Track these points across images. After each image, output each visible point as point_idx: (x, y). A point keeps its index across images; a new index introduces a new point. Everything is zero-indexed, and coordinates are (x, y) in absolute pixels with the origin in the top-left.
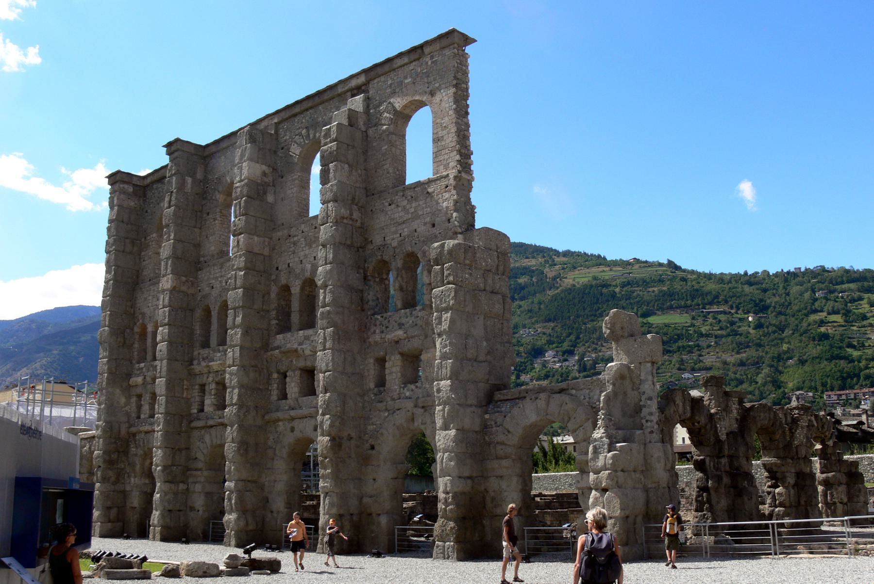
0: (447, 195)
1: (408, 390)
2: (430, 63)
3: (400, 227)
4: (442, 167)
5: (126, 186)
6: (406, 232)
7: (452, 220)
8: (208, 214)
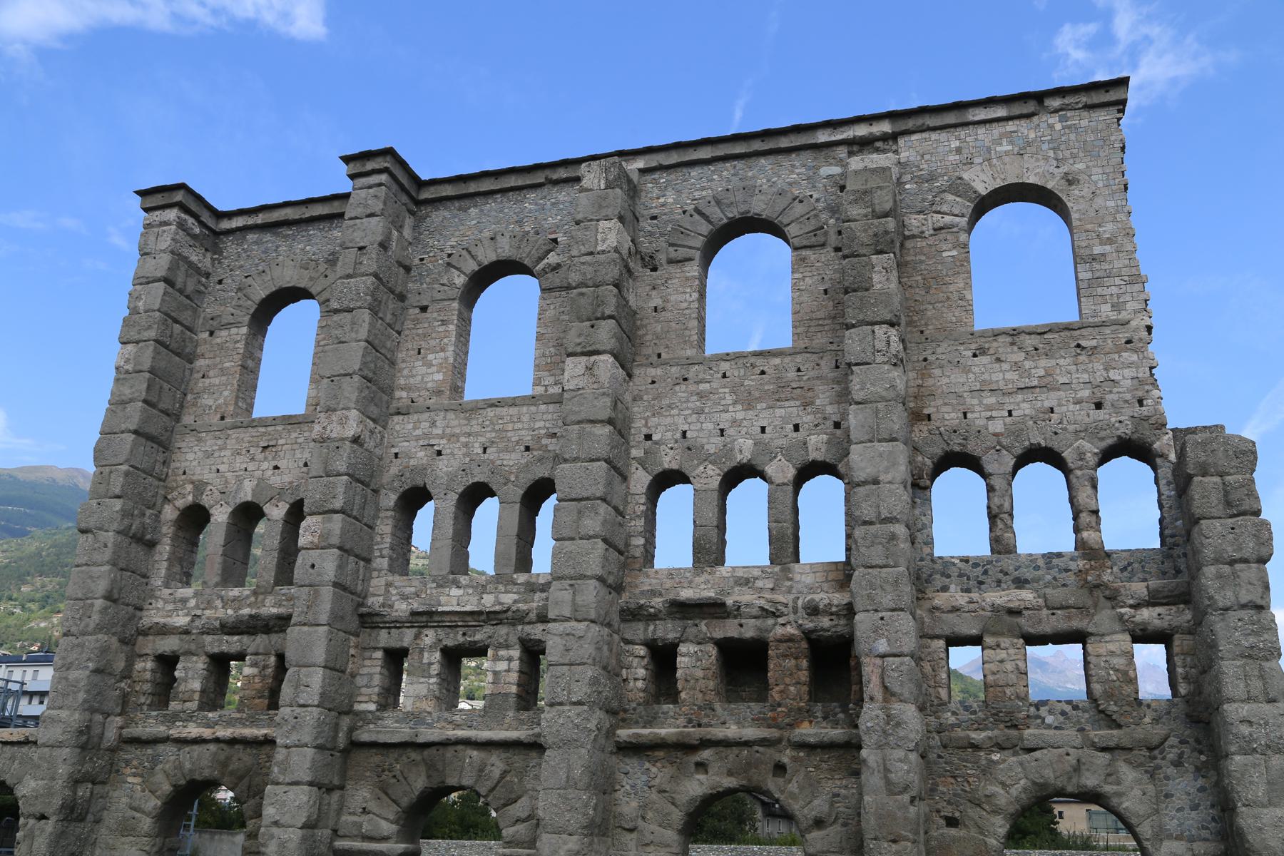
1: (1050, 712)
2: (1058, 126)
3: (1006, 399)
5: (191, 220)
6: (1026, 409)
7: (1148, 402)
8: (424, 309)
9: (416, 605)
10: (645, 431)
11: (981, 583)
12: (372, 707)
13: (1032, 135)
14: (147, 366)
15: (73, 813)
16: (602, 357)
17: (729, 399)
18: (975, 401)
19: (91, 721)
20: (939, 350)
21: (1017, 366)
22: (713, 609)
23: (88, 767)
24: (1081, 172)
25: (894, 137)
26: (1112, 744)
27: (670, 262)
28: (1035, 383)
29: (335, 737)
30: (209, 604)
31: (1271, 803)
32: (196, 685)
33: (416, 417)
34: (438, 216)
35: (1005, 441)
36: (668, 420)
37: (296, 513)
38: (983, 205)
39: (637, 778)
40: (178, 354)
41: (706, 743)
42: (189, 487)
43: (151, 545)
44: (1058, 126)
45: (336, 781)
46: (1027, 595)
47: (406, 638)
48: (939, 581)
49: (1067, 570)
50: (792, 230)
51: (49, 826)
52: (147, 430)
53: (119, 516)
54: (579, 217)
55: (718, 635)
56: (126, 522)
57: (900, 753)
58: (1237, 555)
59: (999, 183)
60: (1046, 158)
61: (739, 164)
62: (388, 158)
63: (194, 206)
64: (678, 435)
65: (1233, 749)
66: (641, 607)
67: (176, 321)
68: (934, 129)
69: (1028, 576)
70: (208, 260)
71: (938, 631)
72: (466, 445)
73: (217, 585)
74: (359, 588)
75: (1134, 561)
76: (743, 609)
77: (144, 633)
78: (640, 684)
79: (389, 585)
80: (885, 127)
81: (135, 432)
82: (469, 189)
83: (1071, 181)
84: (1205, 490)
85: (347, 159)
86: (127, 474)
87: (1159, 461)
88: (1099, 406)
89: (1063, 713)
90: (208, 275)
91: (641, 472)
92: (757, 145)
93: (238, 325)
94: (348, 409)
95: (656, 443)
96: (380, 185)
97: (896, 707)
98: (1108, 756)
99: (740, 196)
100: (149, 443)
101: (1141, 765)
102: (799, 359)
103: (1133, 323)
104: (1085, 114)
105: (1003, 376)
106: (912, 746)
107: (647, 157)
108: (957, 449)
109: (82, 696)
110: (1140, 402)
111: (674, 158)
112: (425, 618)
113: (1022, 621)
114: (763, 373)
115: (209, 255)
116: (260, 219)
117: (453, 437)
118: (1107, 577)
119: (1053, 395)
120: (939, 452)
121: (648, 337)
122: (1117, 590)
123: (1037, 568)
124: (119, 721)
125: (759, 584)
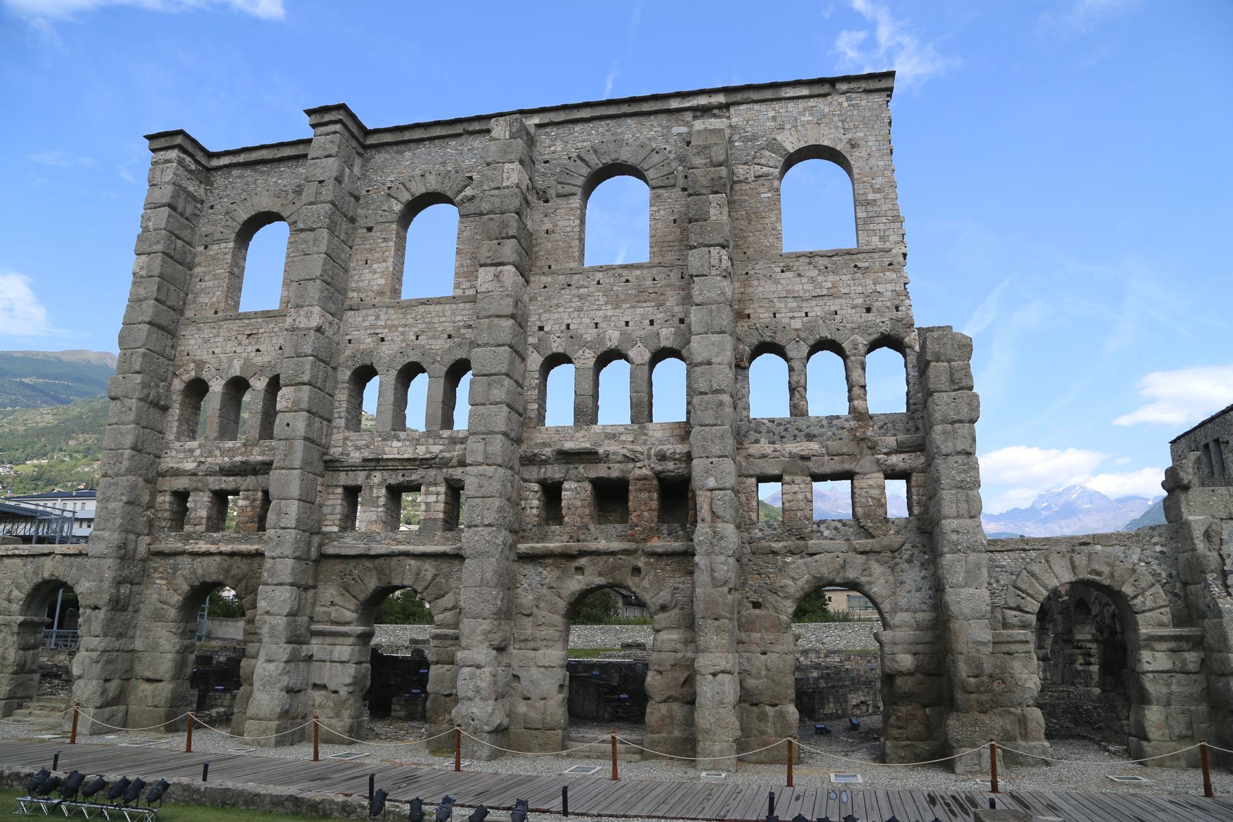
1: (827, 528)
2: (845, 104)
3: (804, 304)
5: (188, 159)
6: (818, 311)
7: (902, 308)
8: (370, 229)
9: (367, 454)
10: (539, 324)
11: (783, 437)
12: (336, 529)
13: (827, 110)
14: (157, 271)
15: (118, 605)
16: (506, 268)
17: (602, 300)
18: (782, 305)
20: (757, 267)
21: (812, 280)
22: (589, 456)
23: (126, 572)
24: (860, 139)
25: (727, 106)
26: (868, 549)
27: (559, 196)
28: (825, 292)
29: (309, 551)
30: (211, 454)
31: (967, 585)
32: (204, 513)
33: (364, 312)
34: (380, 158)
35: (803, 335)
36: (557, 316)
37: (274, 385)
38: (792, 160)
39: (532, 579)
40: (180, 263)
41: (583, 553)
42: (192, 365)
43: (165, 409)
44: (845, 104)
45: (311, 583)
46: (814, 446)
47: (360, 478)
48: (753, 436)
49: (843, 428)
50: (650, 174)
51: (101, 614)
53: (139, 387)
54: (489, 160)
55: (593, 475)
56: (145, 391)
57: (722, 558)
58: (956, 418)
59: (803, 145)
60: (837, 128)
61: (611, 123)
62: (342, 112)
63: (190, 148)
64: (564, 327)
65: (946, 550)
66: (535, 455)
67: (178, 237)
68: (757, 102)
69: (816, 432)
70: (202, 190)
71: (751, 472)
72: (403, 333)
73: (216, 439)
75: (890, 421)
76: (611, 456)
77: (163, 475)
78: (535, 511)
79: (346, 439)
81: (150, 323)
82: (405, 137)
83: (853, 145)
84: (938, 372)
85: (309, 112)
86: (144, 355)
87: (908, 350)
88: (868, 310)
89: (836, 529)
90: (202, 202)
91: (535, 354)
92: (625, 109)
93: (226, 240)
94: (312, 306)
95: (547, 333)
96: (335, 132)
97: (720, 526)
98: (864, 557)
99: (612, 147)
100: (161, 332)
101: (886, 562)
102: (654, 271)
103: (894, 251)
104: (864, 96)
105: (802, 287)
106: (731, 553)
107: (542, 115)
108: (768, 340)
109: (119, 521)
110: (897, 308)
111: (562, 116)
112: (373, 464)
113: (810, 464)
114: (627, 281)
115: (203, 186)
116: (242, 158)
117: (393, 328)
118: (869, 433)
119: (838, 301)
120: (755, 342)
121: (541, 253)
122: (876, 442)
123: (822, 427)
124: (147, 539)
125: (623, 438)
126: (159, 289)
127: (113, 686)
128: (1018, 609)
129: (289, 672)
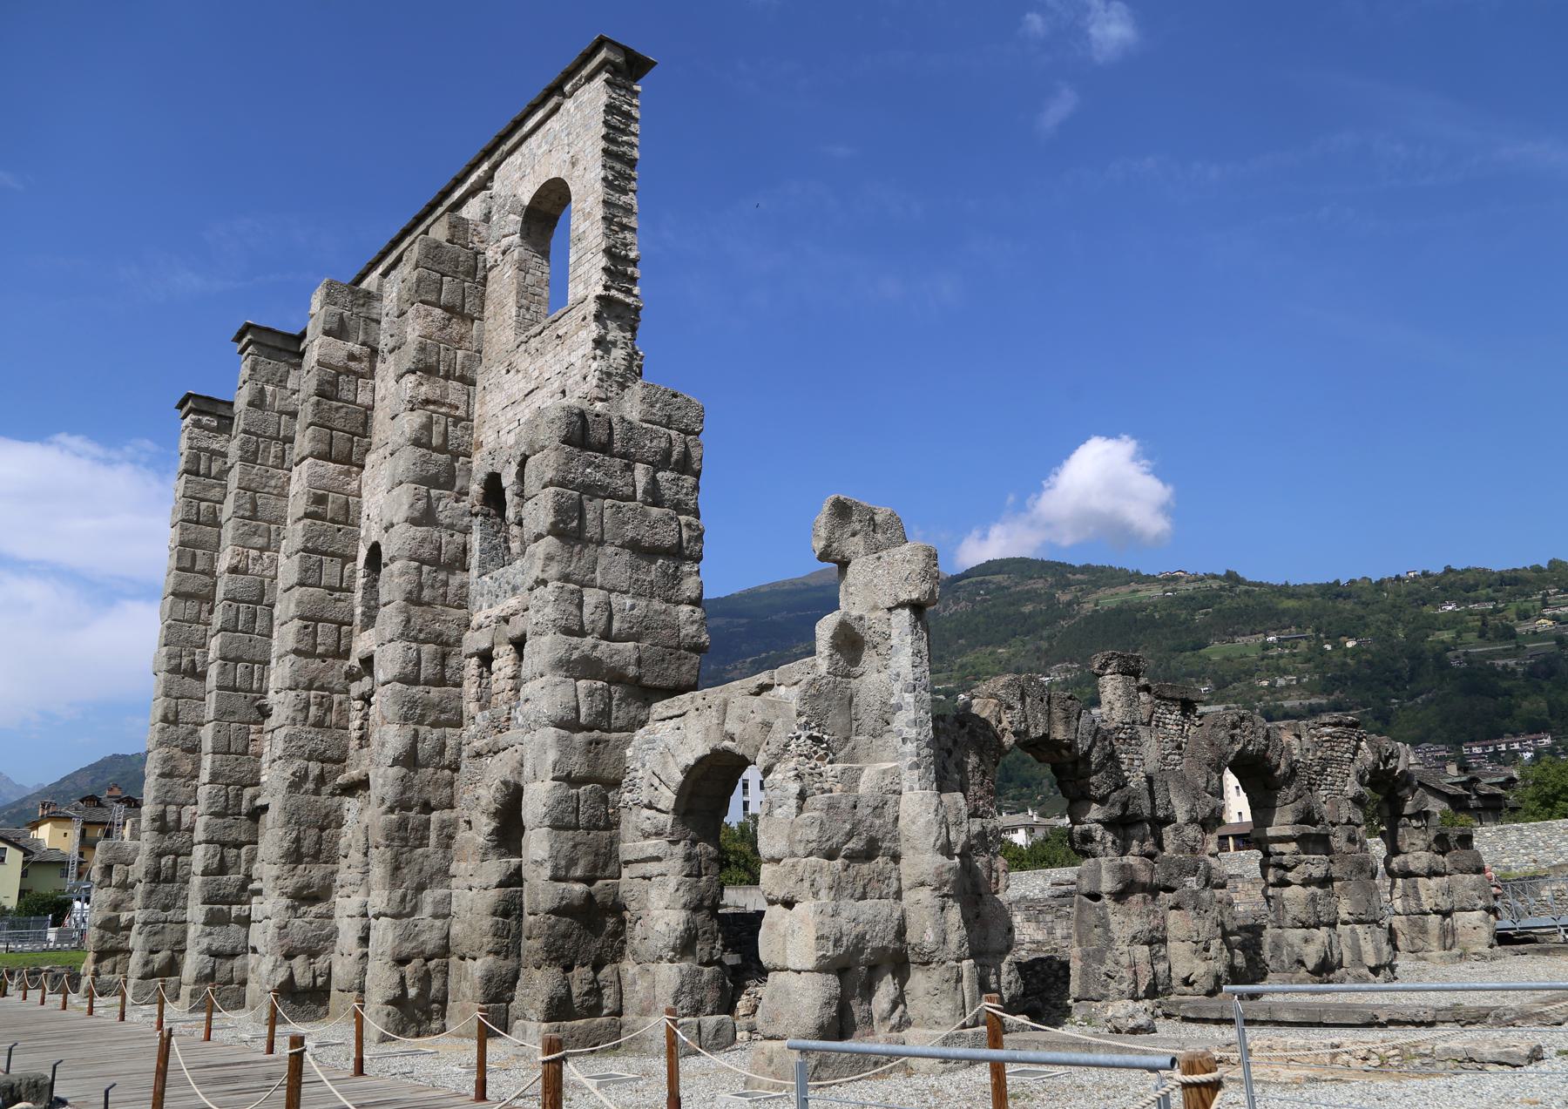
0: (583, 334)
3: (519, 409)
4: (581, 287)
15: (155, 876)
19: (164, 811)
45: (243, 838)
52: (183, 589)
74: (255, 686)
80: (485, 166)
81: (173, 594)
126: (179, 558)
127: (159, 959)
128: (650, 806)
129: (210, 934)
